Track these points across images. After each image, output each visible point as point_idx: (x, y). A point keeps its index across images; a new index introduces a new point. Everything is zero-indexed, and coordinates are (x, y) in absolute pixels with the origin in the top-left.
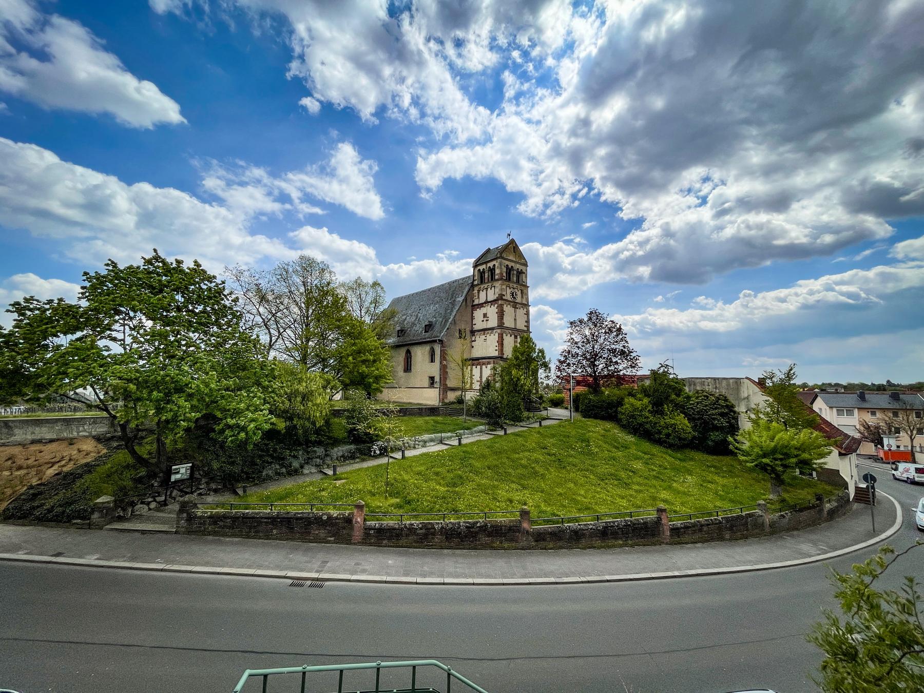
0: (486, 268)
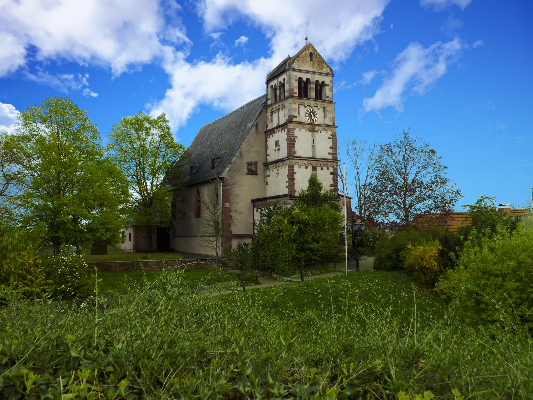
0: (278, 83)
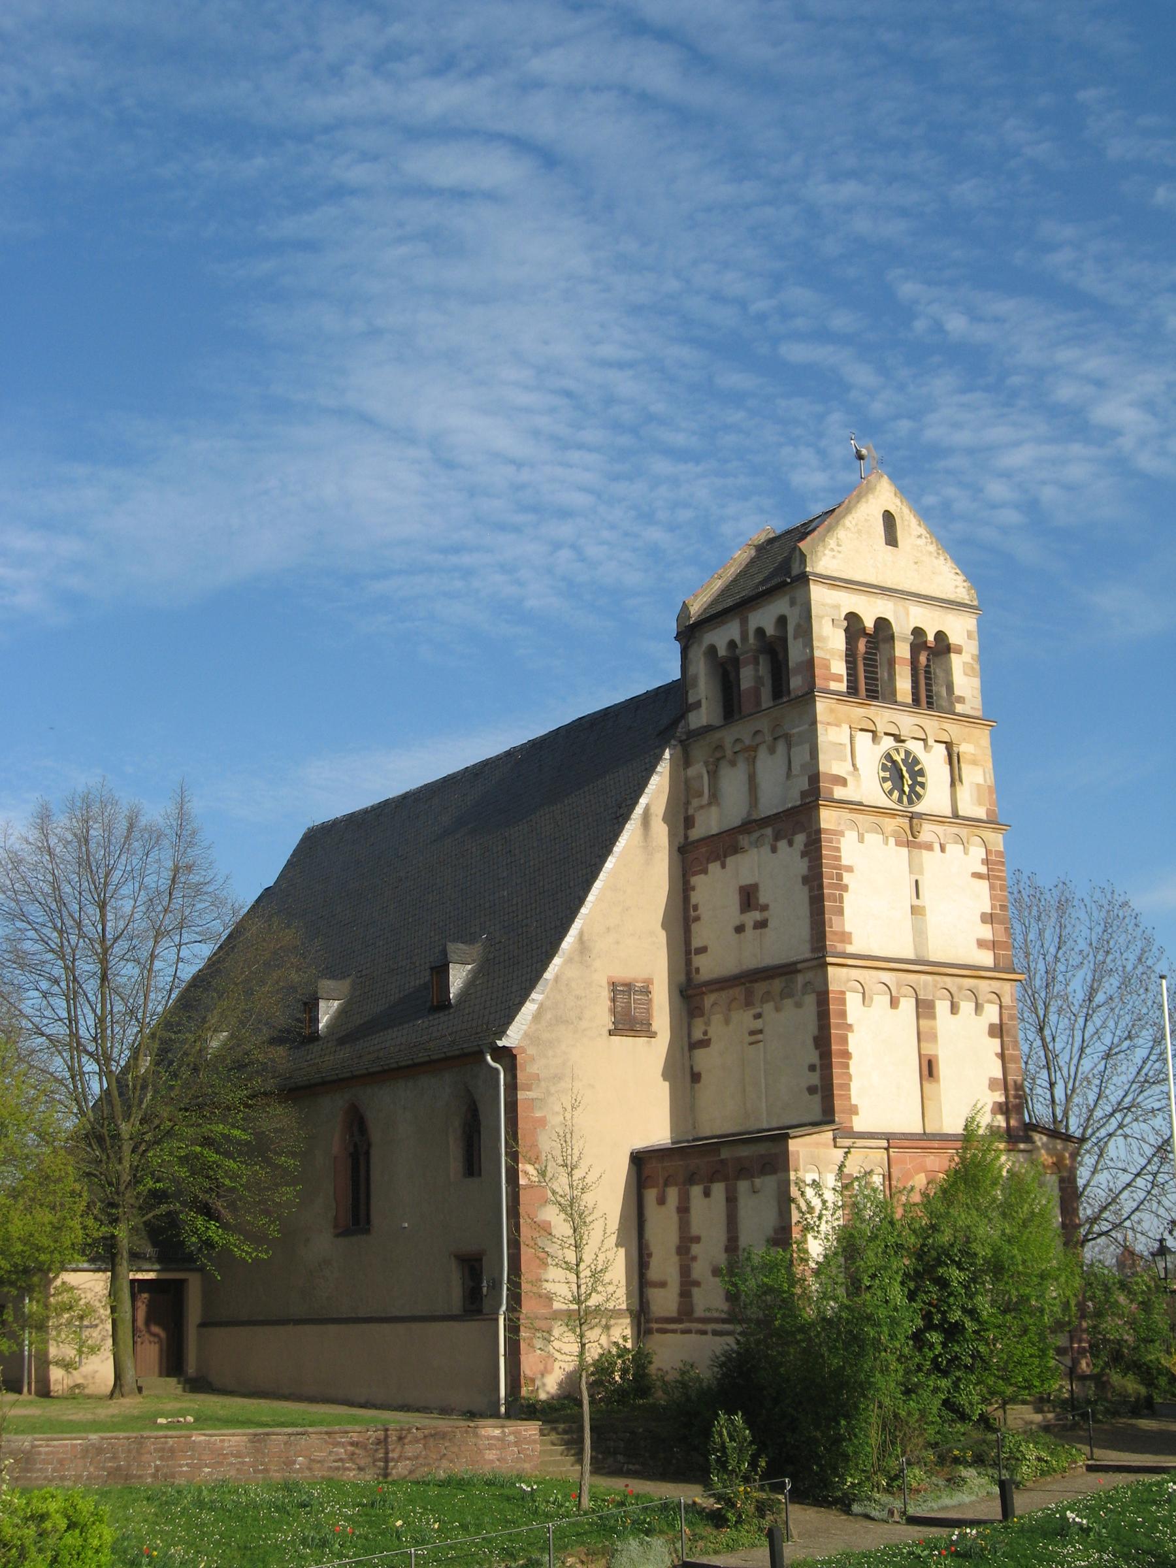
0: (744, 636)
